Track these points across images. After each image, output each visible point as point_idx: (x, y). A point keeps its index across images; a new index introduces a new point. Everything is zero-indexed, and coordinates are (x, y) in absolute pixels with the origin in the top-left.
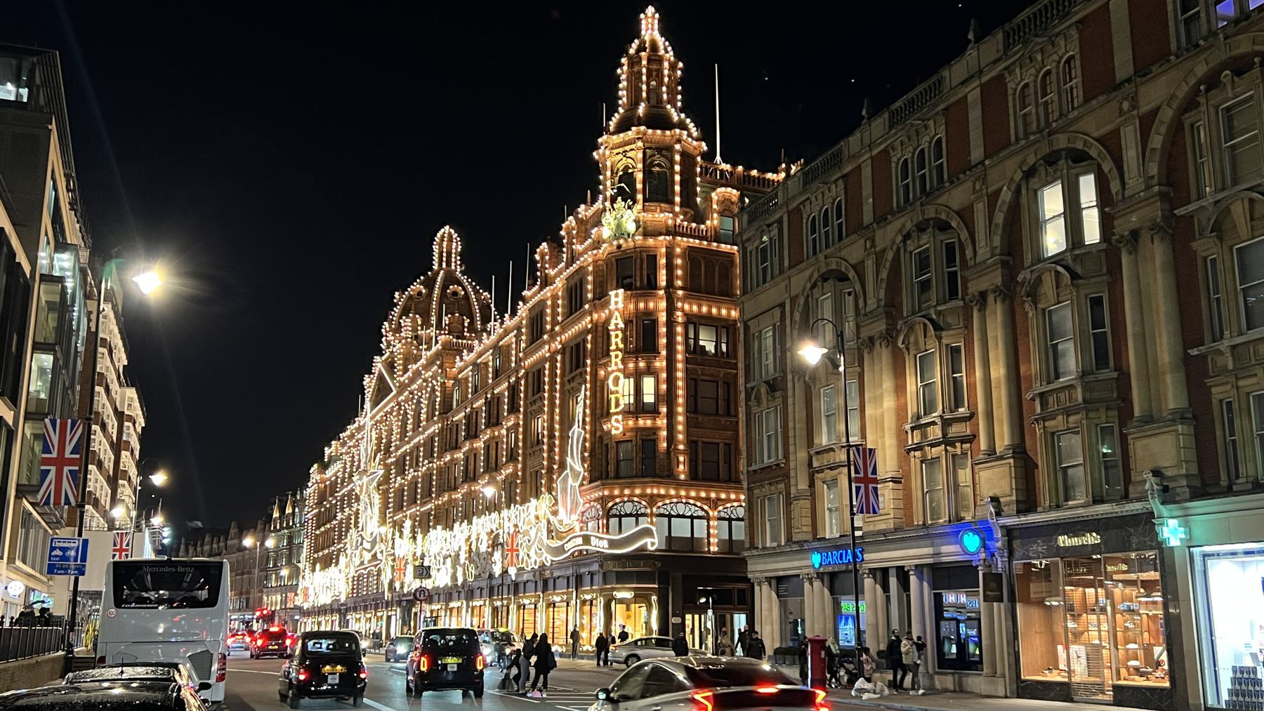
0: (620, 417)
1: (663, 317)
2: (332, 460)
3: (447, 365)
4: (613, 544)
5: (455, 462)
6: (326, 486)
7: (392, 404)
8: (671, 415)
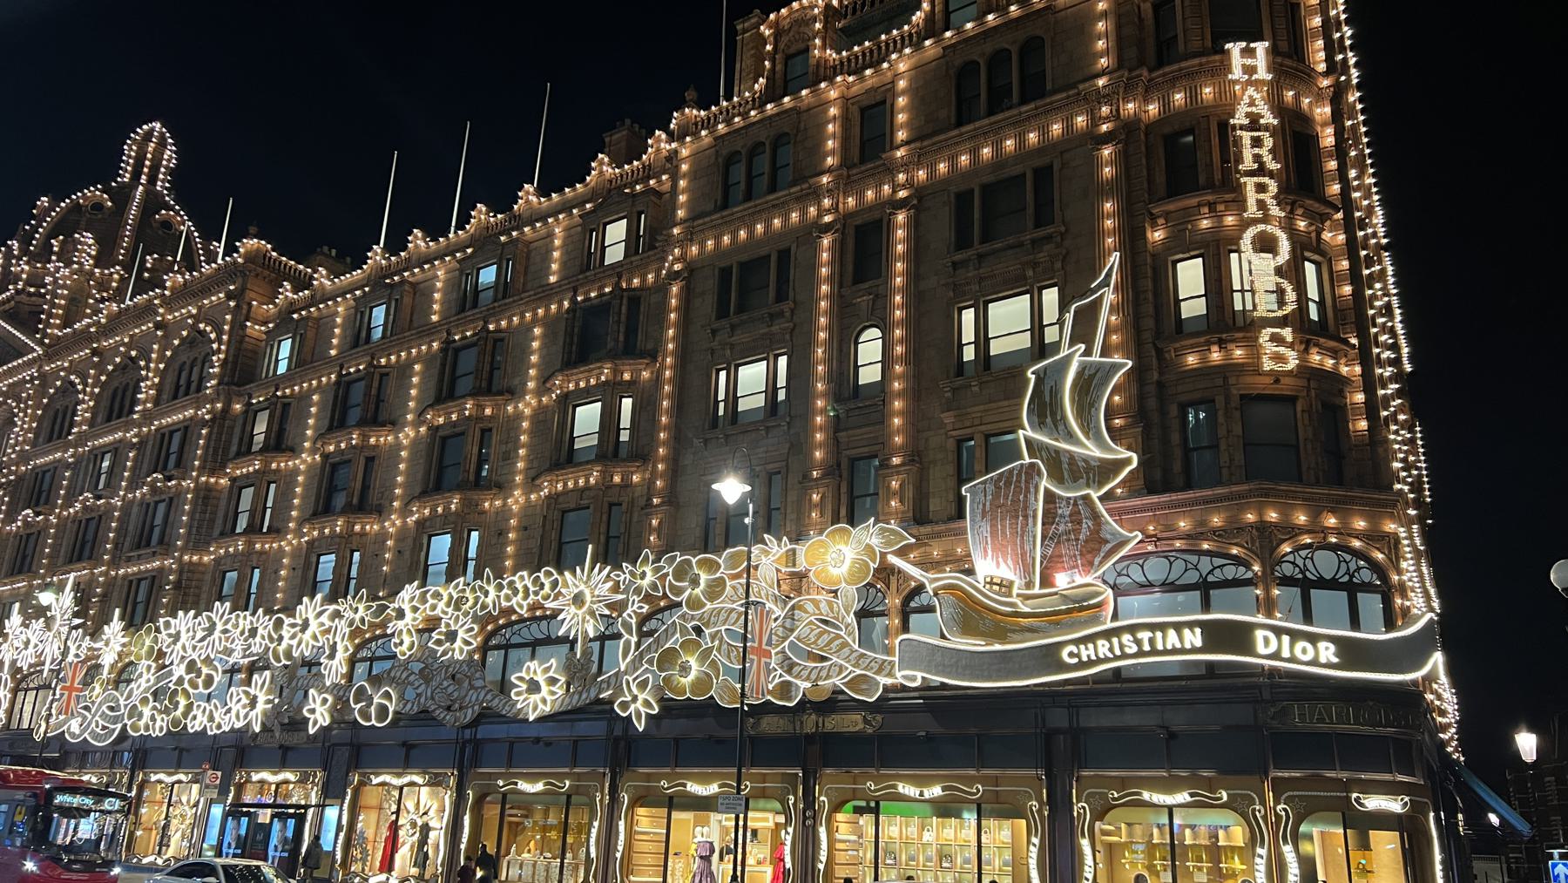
0: (1287, 333)
3: (252, 295)
4: (1351, 653)
7: (26, 375)
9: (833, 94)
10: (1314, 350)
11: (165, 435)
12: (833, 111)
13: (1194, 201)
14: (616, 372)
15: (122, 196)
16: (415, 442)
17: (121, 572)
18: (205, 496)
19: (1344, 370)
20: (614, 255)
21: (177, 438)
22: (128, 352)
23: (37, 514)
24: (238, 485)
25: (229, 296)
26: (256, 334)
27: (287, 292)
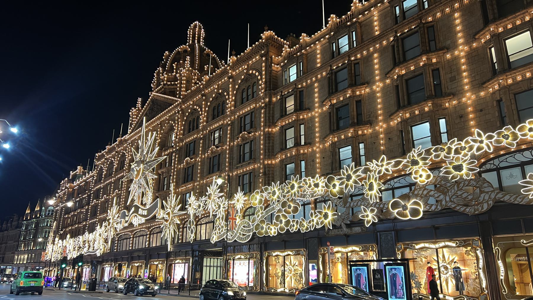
2: (75, 177)
5: (301, 122)
6: (74, 190)
15: (192, 46)
18: (269, 137)
23: (191, 159)
24: (284, 130)
25: (262, 56)
26: (275, 69)
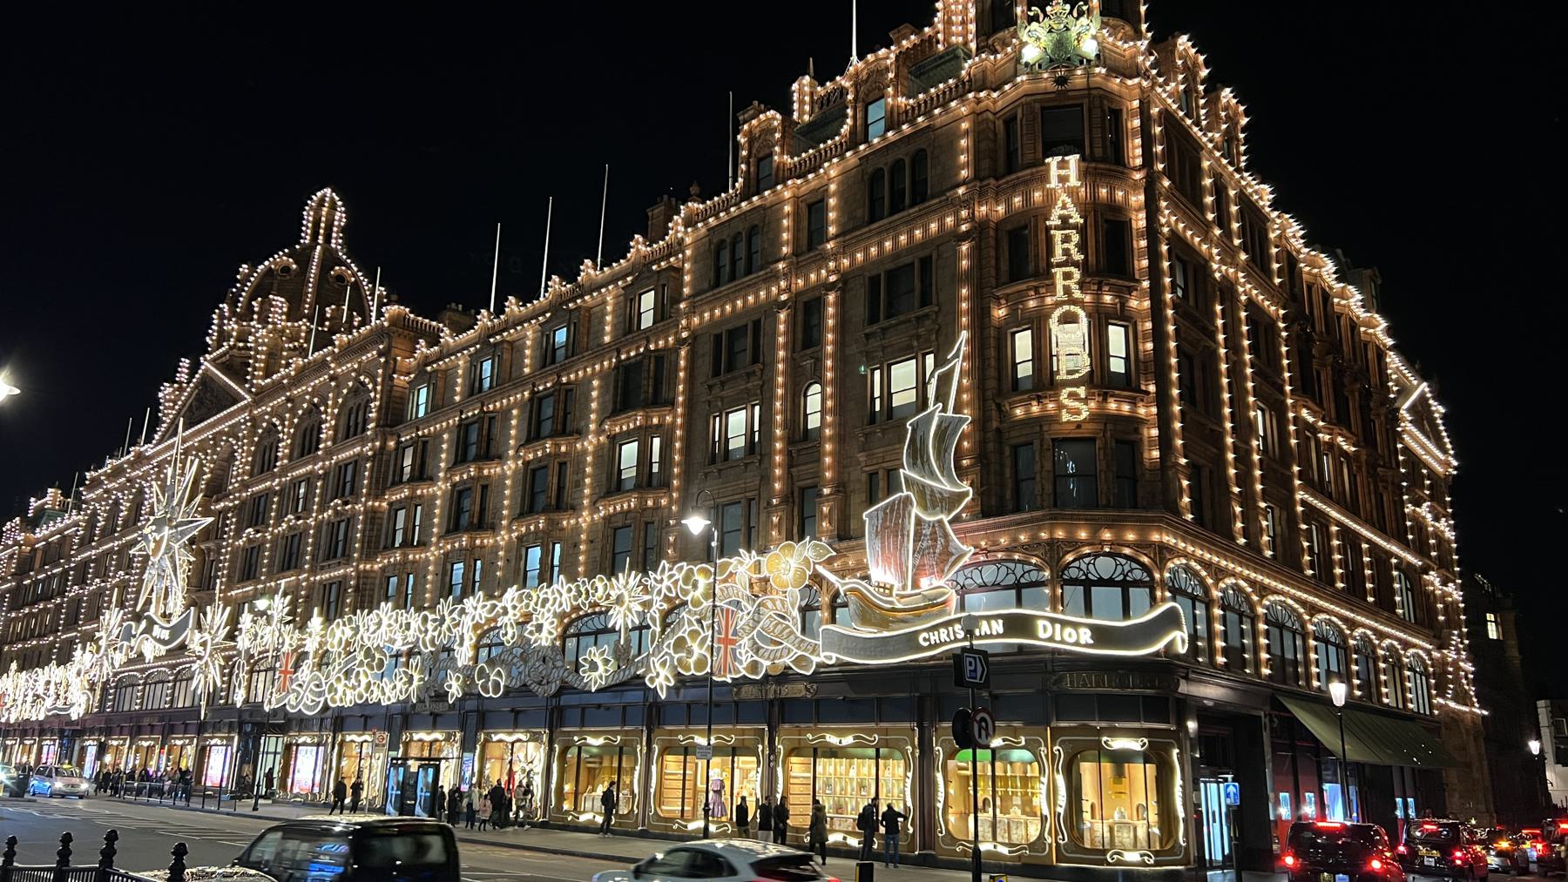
0: (1082, 391)
1: (1140, 221)
2: (41, 516)
3: (397, 351)
4: (1102, 635)
5: (418, 501)
6: (34, 550)
7: (240, 418)
8: (1162, 400)
9: (787, 194)
10: (1111, 400)
11: (341, 468)
12: (787, 208)
13: (1024, 287)
14: (648, 418)
15: (304, 258)
16: (516, 472)
17: (318, 578)
18: (372, 515)
19: (1142, 411)
20: (647, 321)
21: (350, 468)
22: (311, 400)
23: (258, 532)
24: (394, 508)
25: (380, 354)
26: (402, 384)
27: (422, 348)
